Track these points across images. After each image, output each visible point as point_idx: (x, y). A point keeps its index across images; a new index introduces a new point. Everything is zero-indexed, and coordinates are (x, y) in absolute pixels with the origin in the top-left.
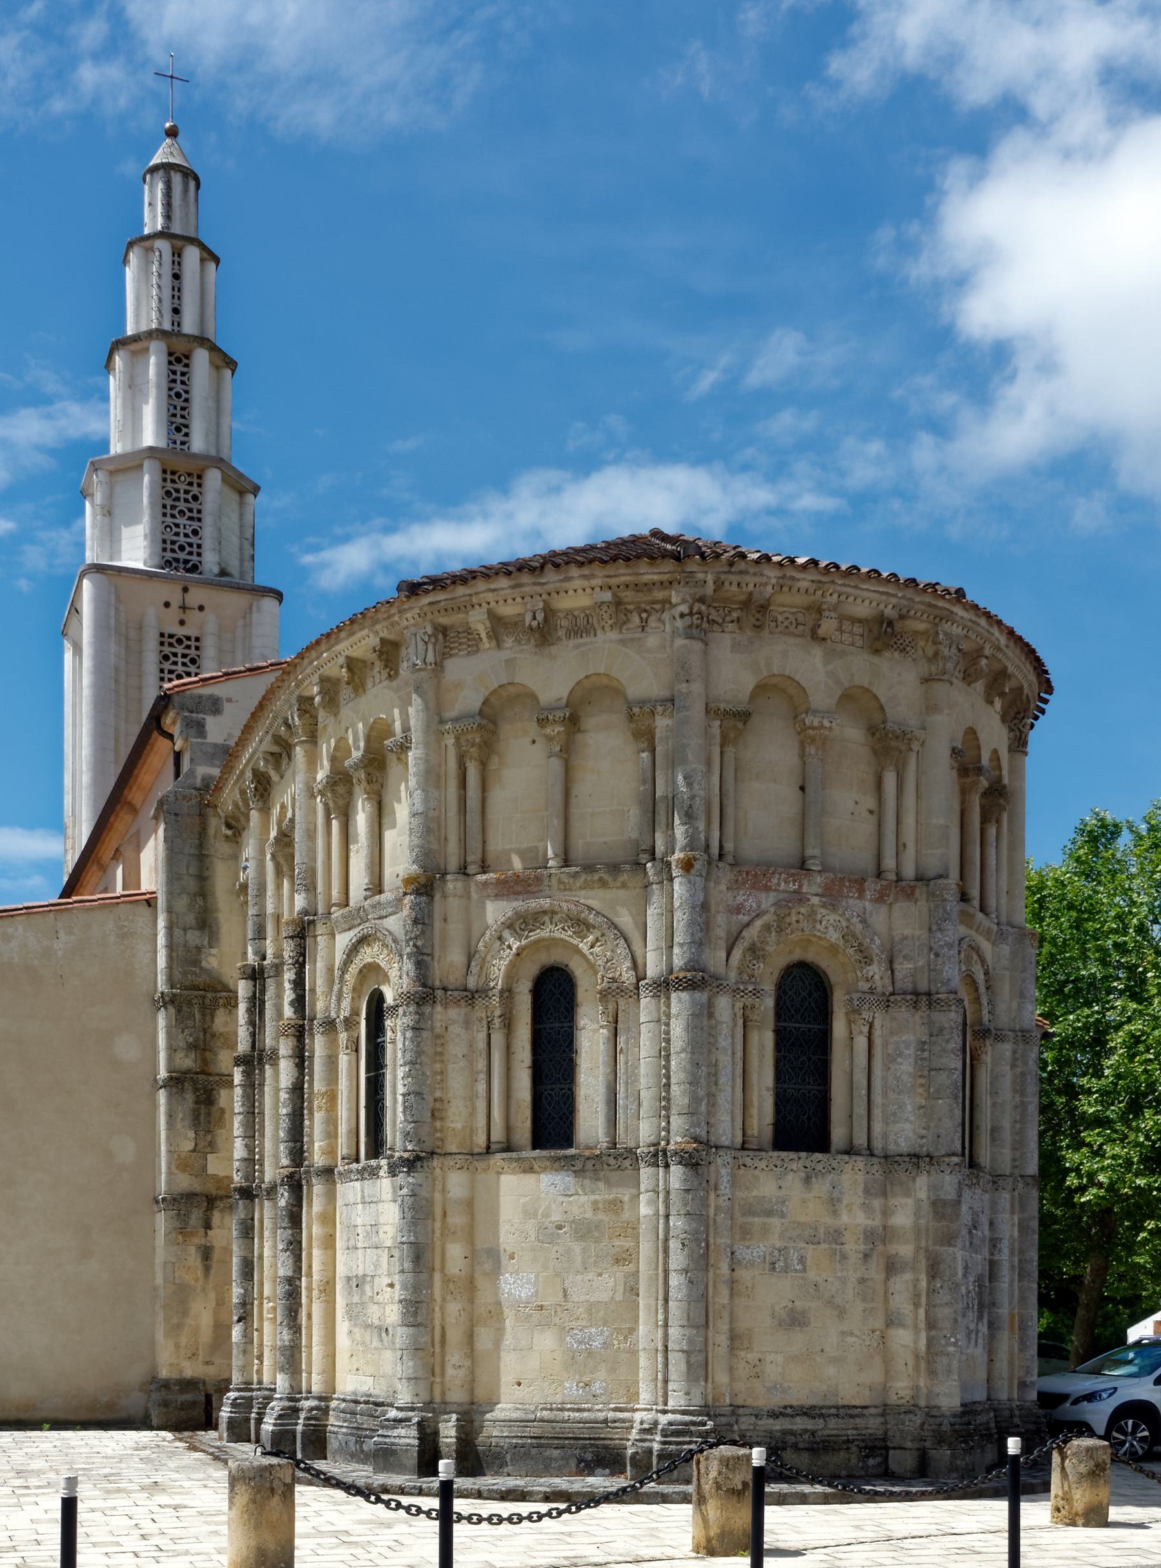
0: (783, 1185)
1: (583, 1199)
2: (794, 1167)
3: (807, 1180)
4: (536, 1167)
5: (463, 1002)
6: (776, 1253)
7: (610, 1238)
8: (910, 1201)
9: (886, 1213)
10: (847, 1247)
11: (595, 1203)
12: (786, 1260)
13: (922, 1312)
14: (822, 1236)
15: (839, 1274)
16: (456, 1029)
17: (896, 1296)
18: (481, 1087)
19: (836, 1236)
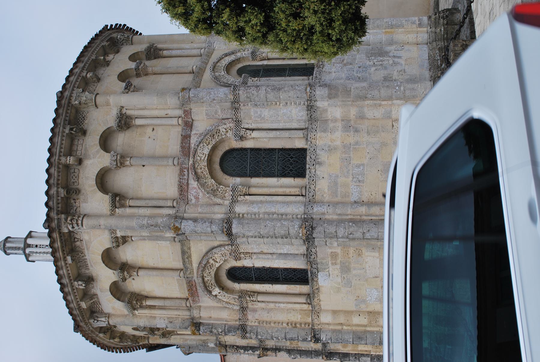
0: (322, 176)
1: (331, 269)
3: (320, 164)
4: (317, 287)
5: (245, 313)
6: (355, 180)
7: (349, 258)
8: (329, 110)
9: (335, 120)
10: (352, 142)
11: (332, 264)
12: (359, 175)
13: (383, 103)
14: (347, 155)
15: (365, 146)
16: (257, 316)
17: (375, 115)
18: (282, 305)
19: (347, 148)
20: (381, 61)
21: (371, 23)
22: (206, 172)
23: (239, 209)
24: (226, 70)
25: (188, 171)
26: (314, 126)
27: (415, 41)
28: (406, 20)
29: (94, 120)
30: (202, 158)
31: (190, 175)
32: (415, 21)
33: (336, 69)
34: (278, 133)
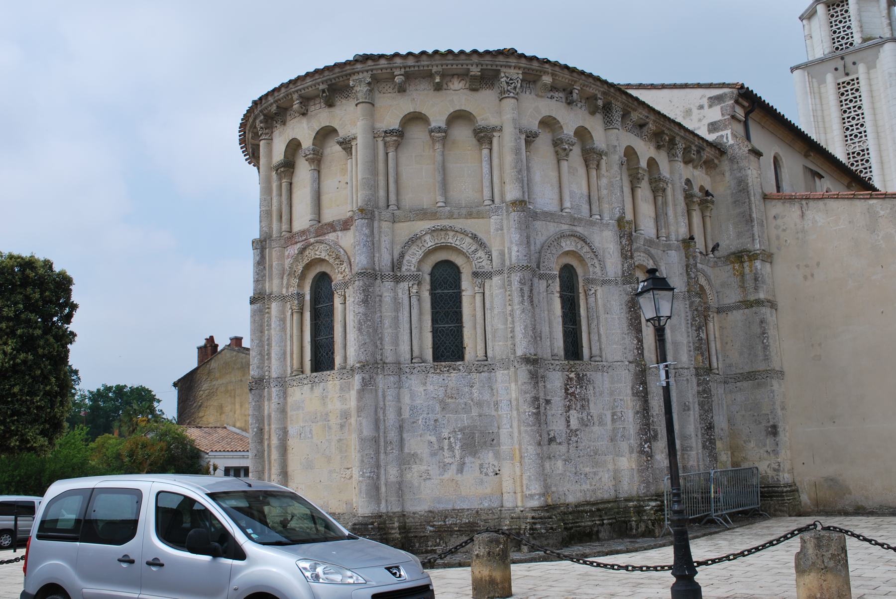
2: (305, 382)
3: (312, 388)
15: (327, 438)
19: (326, 417)
20: (451, 448)
21: (526, 428)
22: (306, 261)
23: (274, 306)
25: (305, 240)
26: (345, 375)
28: (530, 477)
29: (345, 110)
30: (317, 252)
31: (303, 243)
32: (529, 490)
33: (432, 391)
34: (340, 334)
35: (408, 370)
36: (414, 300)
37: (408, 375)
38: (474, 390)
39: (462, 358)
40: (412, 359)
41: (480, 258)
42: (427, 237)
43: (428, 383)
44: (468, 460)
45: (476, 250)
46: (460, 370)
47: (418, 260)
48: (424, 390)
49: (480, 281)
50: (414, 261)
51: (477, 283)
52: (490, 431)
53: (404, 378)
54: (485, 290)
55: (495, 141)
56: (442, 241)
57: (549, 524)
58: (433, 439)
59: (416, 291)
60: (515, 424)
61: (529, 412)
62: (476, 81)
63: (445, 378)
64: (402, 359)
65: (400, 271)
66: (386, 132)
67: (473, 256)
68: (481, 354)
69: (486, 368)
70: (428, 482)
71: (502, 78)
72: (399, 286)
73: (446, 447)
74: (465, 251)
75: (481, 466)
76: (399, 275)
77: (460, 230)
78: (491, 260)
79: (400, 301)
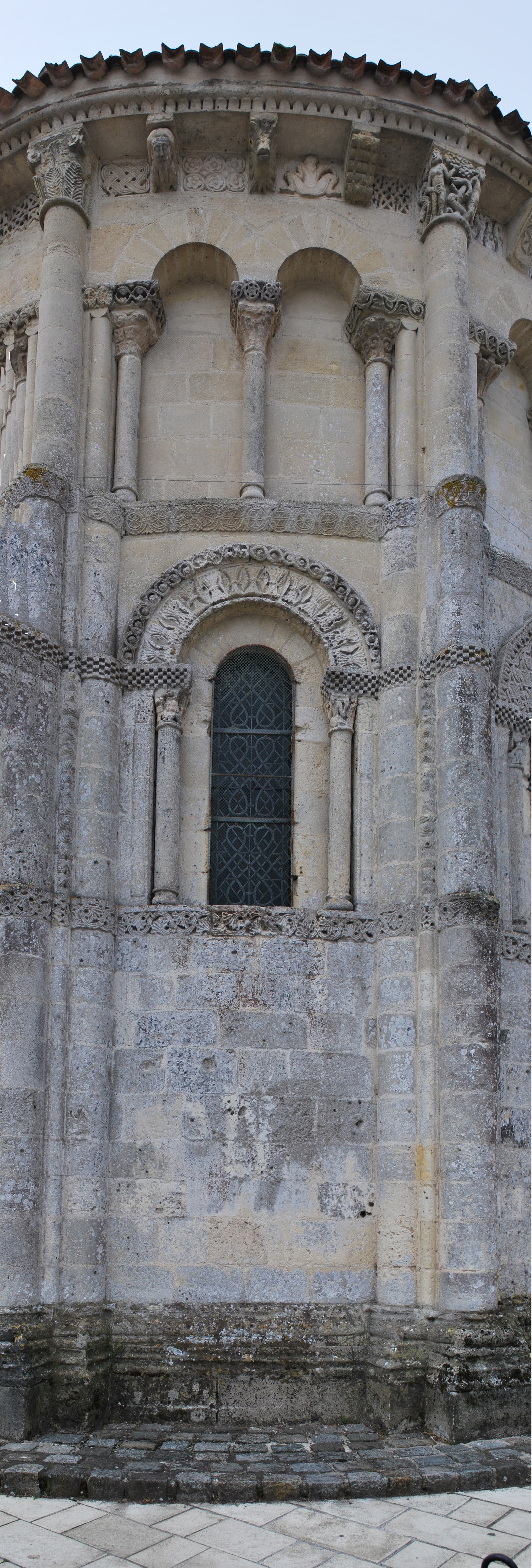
20: (245, 1138)
21: (457, 1093)
24: (247, 601)
27: (383, 1258)
28: (462, 1227)
32: (459, 1262)
33: (201, 982)
35: (138, 922)
36: (167, 737)
37: (138, 936)
38: (315, 988)
39: (288, 901)
40: (152, 895)
41: (350, 642)
42: (212, 578)
43: (191, 957)
44: (290, 1171)
45: (339, 622)
46: (279, 928)
47: (183, 636)
48: (181, 978)
49: (346, 700)
50: (172, 636)
51: (339, 704)
52: (354, 1099)
53: (126, 942)
54: (359, 726)
55: (405, 342)
56: (250, 590)
57: (508, 1360)
58: (198, 1110)
59: (172, 714)
60: (427, 1081)
61: (470, 1047)
62: (365, 166)
63: (239, 947)
64: (124, 894)
65: (134, 659)
66: (116, 291)
67: (330, 634)
68: (338, 891)
69: (350, 930)
70: (176, 1225)
71: (434, 165)
72: (127, 699)
73: (231, 1135)
74: (310, 621)
75: (324, 1190)
76: (129, 668)
77: (298, 564)
78: (378, 649)
79: (129, 739)
